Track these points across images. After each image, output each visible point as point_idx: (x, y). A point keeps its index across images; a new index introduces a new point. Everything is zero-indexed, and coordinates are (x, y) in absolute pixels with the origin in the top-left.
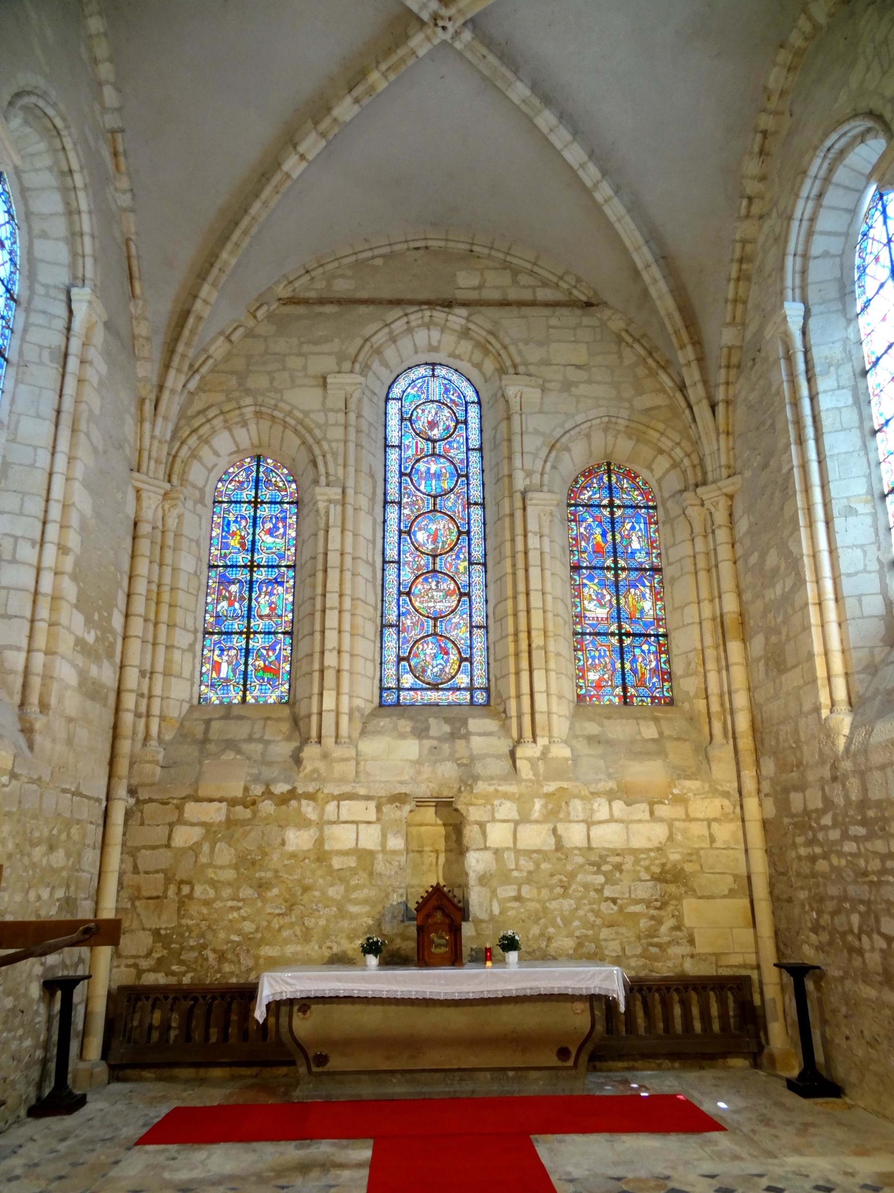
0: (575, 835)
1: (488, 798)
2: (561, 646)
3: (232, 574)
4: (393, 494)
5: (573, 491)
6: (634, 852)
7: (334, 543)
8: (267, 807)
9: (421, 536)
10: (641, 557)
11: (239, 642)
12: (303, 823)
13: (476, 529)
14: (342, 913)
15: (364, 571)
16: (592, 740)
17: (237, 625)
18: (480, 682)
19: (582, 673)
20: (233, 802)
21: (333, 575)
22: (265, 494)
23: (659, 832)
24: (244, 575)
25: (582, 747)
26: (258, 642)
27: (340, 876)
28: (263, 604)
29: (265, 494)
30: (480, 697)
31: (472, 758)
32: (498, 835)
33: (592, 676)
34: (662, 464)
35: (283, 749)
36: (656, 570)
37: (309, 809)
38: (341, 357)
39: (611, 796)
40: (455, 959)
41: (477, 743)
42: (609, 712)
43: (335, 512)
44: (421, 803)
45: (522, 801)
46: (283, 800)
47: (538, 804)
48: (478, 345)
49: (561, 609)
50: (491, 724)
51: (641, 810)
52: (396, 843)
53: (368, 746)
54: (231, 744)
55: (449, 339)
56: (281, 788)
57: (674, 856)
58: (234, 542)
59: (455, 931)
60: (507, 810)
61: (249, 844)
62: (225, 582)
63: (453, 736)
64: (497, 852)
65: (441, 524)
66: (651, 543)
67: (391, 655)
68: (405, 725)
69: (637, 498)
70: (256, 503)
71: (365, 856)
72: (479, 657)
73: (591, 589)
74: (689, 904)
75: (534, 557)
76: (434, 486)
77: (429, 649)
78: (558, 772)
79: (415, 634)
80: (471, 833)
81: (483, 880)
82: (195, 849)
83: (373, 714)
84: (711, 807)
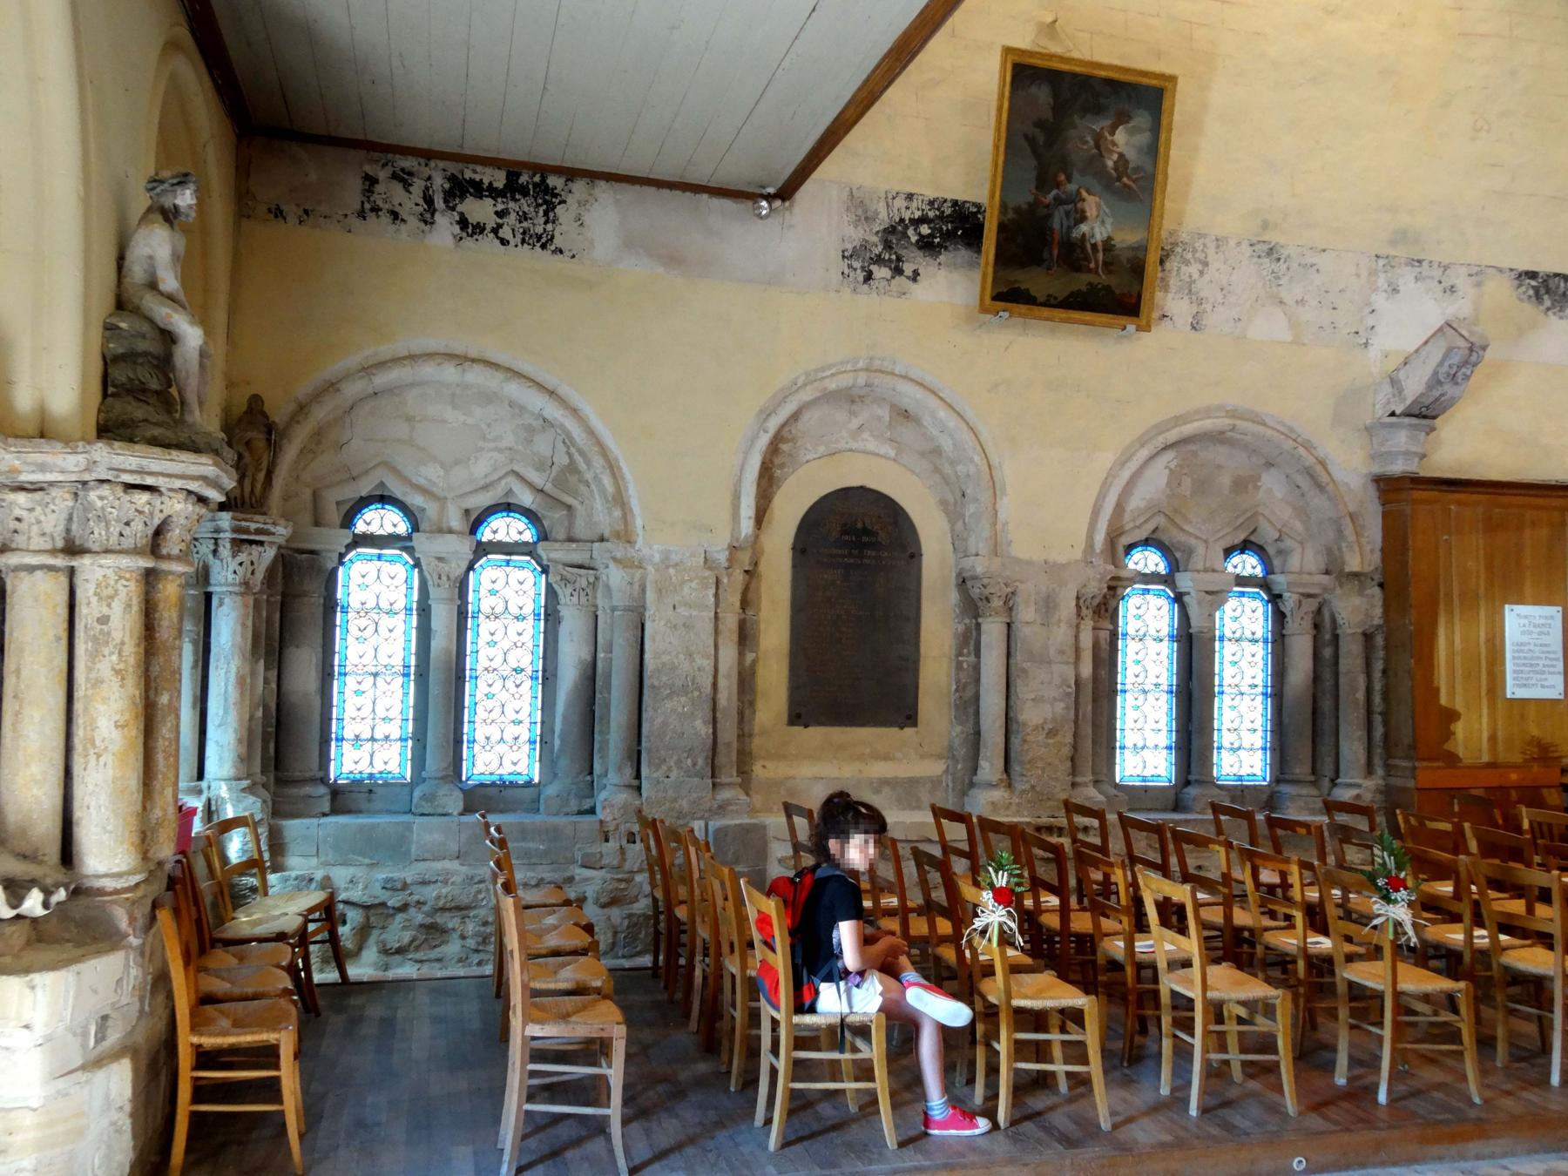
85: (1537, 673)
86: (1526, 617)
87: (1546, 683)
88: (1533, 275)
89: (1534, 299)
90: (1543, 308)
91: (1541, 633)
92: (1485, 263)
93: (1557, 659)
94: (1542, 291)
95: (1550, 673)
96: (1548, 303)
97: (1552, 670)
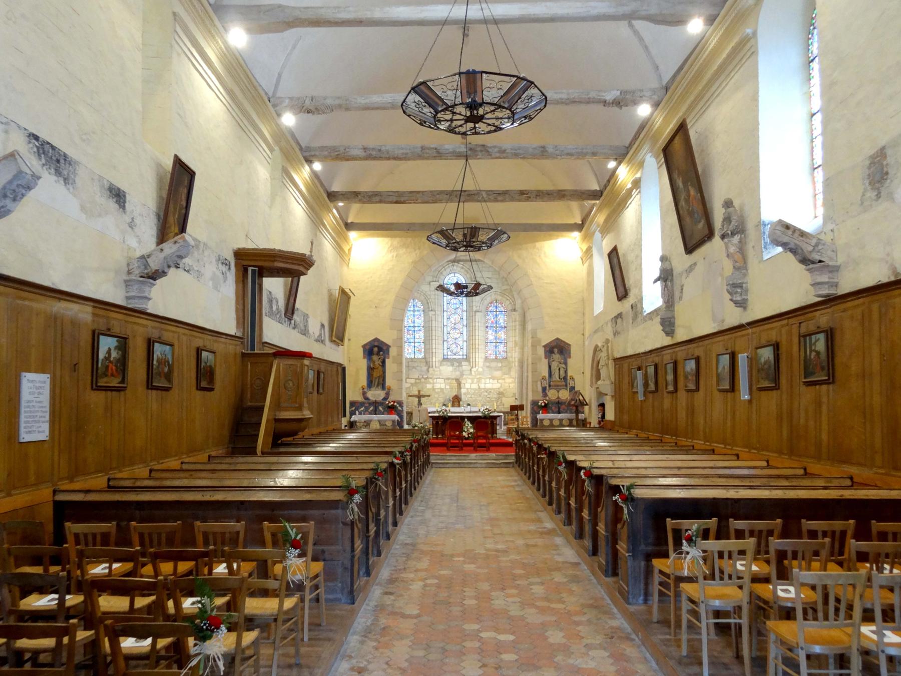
0: (482, 386)
1: (466, 379)
2: (482, 347)
3: (410, 328)
4: (445, 309)
5: (487, 308)
6: (494, 389)
7: (433, 325)
8: (423, 380)
9: (452, 319)
10: (502, 325)
11: (413, 344)
12: (430, 383)
13: (465, 318)
14: (438, 399)
15: (440, 329)
16: (488, 367)
17: (412, 341)
18: (465, 353)
19: (487, 352)
20: (416, 379)
21: (434, 332)
22: (416, 309)
23: (498, 385)
24: (413, 329)
25: (485, 369)
26: (417, 344)
27: (438, 393)
28: (417, 336)
29: (416, 309)
30: (465, 357)
31: (463, 371)
32: (468, 386)
33: (489, 352)
34: (508, 302)
35: (425, 368)
36: (505, 327)
37: (431, 380)
38: (433, 277)
39: (490, 378)
40: (459, 406)
41: (464, 367)
42: (492, 360)
43: (433, 317)
44: (452, 379)
45: (472, 379)
46: (426, 379)
47: (475, 380)
48: (466, 271)
49: (482, 338)
50: (467, 363)
51: (496, 381)
52: (448, 387)
53: (442, 368)
54: (414, 367)
55: (459, 269)
56: (425, 376)
57: (502, 390)
58: (410, 321)
59: (459, 402)
60: (470, 381)
61: (420, 387)
62: (408, 331)
63: (459, 366)
64: (467, 389)
65: (456, 316)
66: (505, 320)
67: (445, 348)
68: (449, 363)
69: (502, 309)
70: (414, 311)
71: (442, 389)
72: (465, 348)
73: (490, 332)
74: (504, 399)
75: (477, 327)
76: (455, 306)
77: (454, 346)
78: (479, 374)
79: (451, 343)
80: (462, 385)
81: (465, 394)
82: (409, 388)
83: (442, 361)
84: (510, 380)
85: (35, 422)
86: (32, 381)
87: (40, 429)
88: (36, 138)
89: (36, 154)
90: (41, 163)
91: (39, 393)
92: (10, 117)
93: (45, 412)
94: (41, 151)
95: (43, 422)
96: (43, 161)
97: (43, 419)
